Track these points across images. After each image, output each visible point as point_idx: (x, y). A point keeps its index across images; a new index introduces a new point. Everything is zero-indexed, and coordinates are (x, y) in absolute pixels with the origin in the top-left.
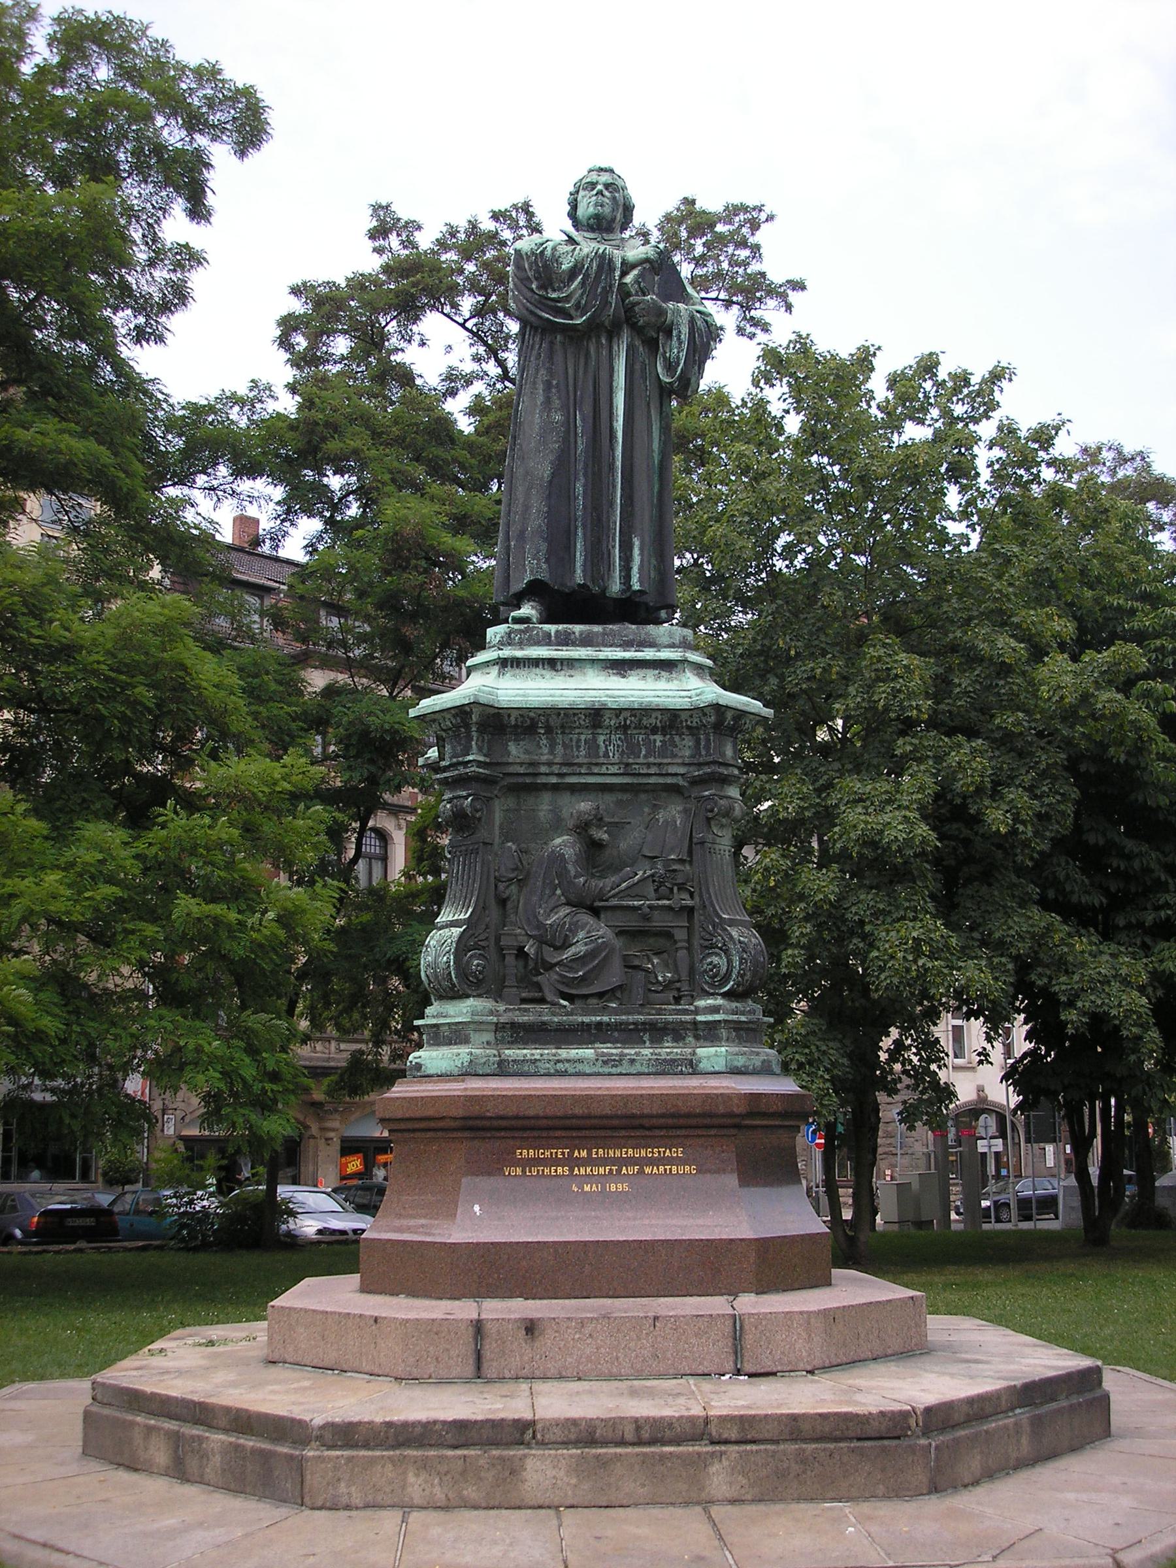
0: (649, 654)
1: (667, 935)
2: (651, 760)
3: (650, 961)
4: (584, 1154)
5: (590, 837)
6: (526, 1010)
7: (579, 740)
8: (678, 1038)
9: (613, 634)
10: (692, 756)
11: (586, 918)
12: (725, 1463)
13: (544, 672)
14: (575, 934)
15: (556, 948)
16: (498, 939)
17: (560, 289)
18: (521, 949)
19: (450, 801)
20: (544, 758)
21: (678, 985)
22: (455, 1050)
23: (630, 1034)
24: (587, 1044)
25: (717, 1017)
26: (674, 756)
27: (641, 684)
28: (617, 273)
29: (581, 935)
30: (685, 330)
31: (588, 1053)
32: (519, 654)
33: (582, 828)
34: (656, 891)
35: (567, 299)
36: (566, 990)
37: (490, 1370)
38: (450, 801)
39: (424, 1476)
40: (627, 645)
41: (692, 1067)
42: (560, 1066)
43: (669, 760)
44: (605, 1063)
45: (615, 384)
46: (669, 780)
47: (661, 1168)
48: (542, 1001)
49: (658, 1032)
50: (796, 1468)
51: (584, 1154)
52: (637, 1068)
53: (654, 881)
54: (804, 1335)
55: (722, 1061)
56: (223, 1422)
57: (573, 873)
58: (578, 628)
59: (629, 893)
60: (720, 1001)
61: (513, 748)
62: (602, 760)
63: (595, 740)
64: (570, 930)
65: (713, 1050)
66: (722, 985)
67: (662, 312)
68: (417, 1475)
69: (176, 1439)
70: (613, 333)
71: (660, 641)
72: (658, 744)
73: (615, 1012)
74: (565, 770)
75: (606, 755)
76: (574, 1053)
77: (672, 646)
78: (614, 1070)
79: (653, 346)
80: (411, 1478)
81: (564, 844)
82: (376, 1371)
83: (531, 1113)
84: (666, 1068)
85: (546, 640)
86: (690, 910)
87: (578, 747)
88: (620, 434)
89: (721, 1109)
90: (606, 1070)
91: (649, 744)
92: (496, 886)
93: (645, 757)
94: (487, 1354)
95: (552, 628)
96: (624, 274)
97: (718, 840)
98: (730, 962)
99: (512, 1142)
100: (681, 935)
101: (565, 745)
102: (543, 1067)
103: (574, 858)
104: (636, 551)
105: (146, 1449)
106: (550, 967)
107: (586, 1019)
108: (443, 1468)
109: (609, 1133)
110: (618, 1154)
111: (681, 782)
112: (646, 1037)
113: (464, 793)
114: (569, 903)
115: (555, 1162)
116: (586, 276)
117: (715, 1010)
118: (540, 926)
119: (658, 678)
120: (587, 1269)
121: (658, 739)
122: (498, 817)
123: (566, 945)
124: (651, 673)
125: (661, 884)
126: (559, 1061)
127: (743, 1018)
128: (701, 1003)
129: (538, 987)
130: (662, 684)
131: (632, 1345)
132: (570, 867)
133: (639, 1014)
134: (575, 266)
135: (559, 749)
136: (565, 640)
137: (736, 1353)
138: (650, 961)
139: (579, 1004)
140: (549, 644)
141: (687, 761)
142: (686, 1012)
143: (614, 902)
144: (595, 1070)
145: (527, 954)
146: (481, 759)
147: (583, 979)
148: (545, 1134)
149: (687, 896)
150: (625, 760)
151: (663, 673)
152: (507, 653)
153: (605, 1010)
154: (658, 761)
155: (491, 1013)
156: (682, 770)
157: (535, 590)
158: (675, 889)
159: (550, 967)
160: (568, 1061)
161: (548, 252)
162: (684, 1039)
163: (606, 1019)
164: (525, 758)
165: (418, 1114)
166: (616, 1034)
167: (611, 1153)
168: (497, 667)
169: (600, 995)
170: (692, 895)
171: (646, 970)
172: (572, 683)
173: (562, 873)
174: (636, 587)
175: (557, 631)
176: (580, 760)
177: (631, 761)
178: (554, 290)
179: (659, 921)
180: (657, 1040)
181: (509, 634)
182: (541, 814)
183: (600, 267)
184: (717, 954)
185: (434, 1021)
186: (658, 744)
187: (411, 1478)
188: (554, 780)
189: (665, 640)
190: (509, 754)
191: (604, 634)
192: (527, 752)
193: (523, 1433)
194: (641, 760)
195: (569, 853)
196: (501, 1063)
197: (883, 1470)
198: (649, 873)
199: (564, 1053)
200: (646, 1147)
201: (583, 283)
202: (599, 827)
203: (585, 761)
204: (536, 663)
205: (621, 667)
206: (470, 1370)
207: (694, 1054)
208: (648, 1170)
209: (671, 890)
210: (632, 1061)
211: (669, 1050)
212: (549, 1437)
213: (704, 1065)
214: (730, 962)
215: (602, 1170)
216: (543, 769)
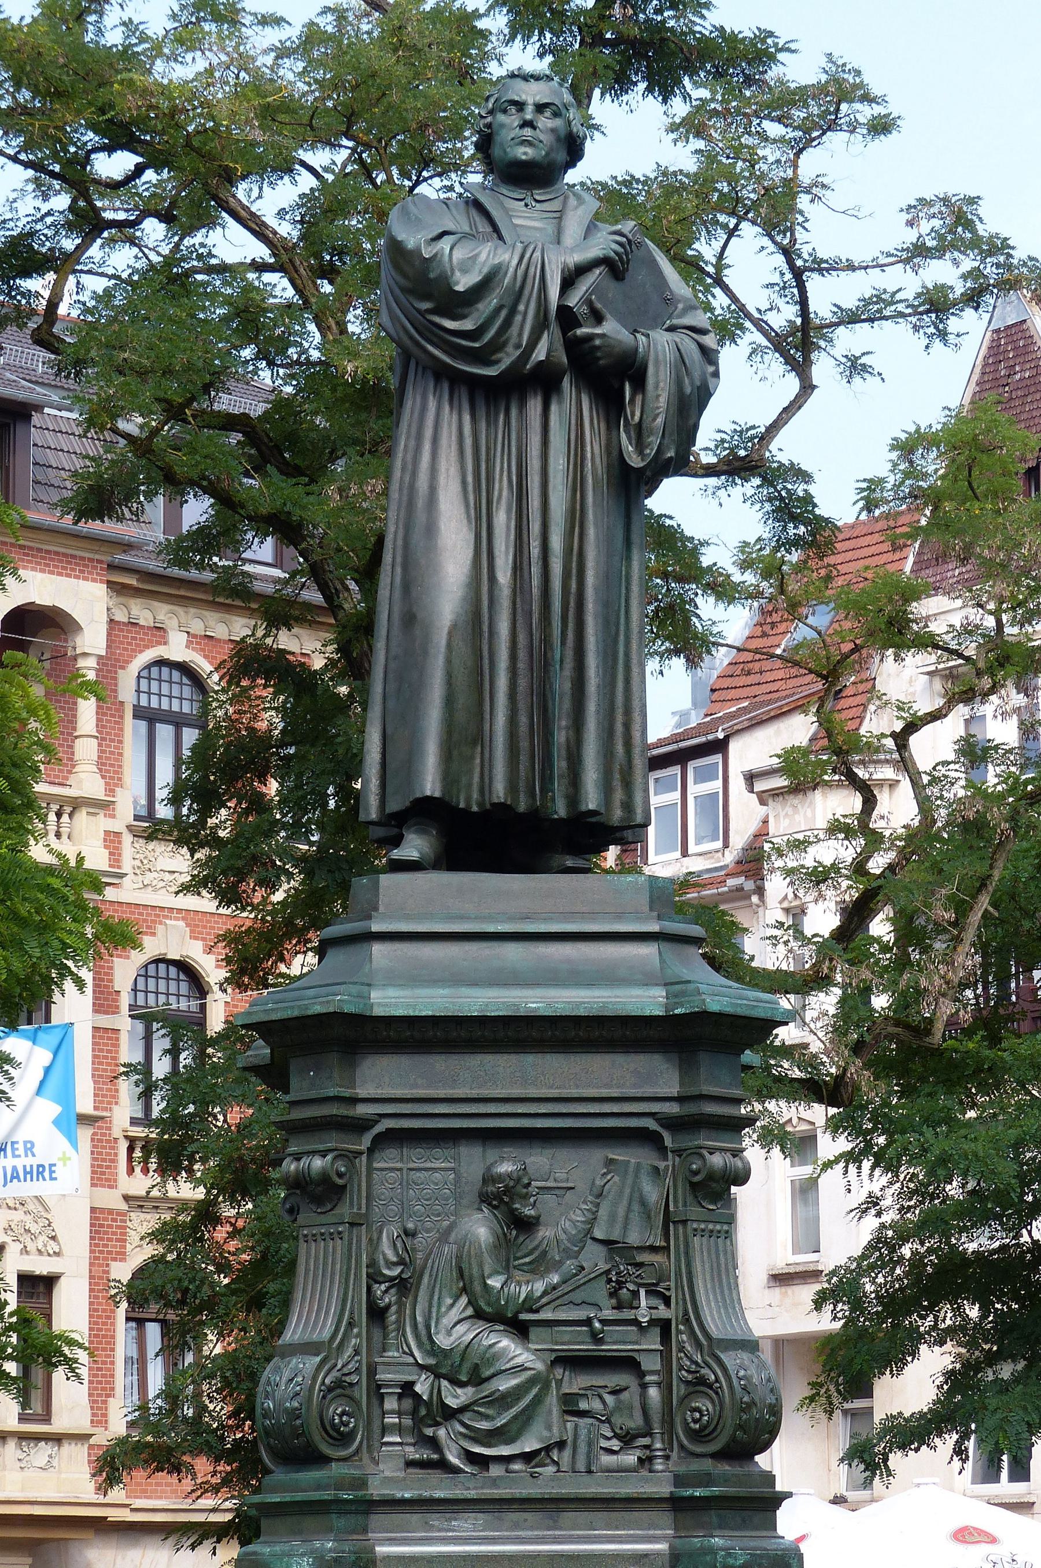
1: (629, 1363)
16: (372, 1371)
18: (407, 1388)
21: (646, 1441)
34: (613, 1294)
36: (478, 1449)
53: (610, 1281)
86: (665, 1326)
92: (369, 1289)
100: (651, 1363)
106: (450, 1414)
111: (651, 1124)
125: (620, 1284)
129: (433, 1443)
145: (417, 1396)
157: (424, 811)
158: (642, 1292)
159: (450, 1414)
169: (527, 1457)
209: (635, 1294)
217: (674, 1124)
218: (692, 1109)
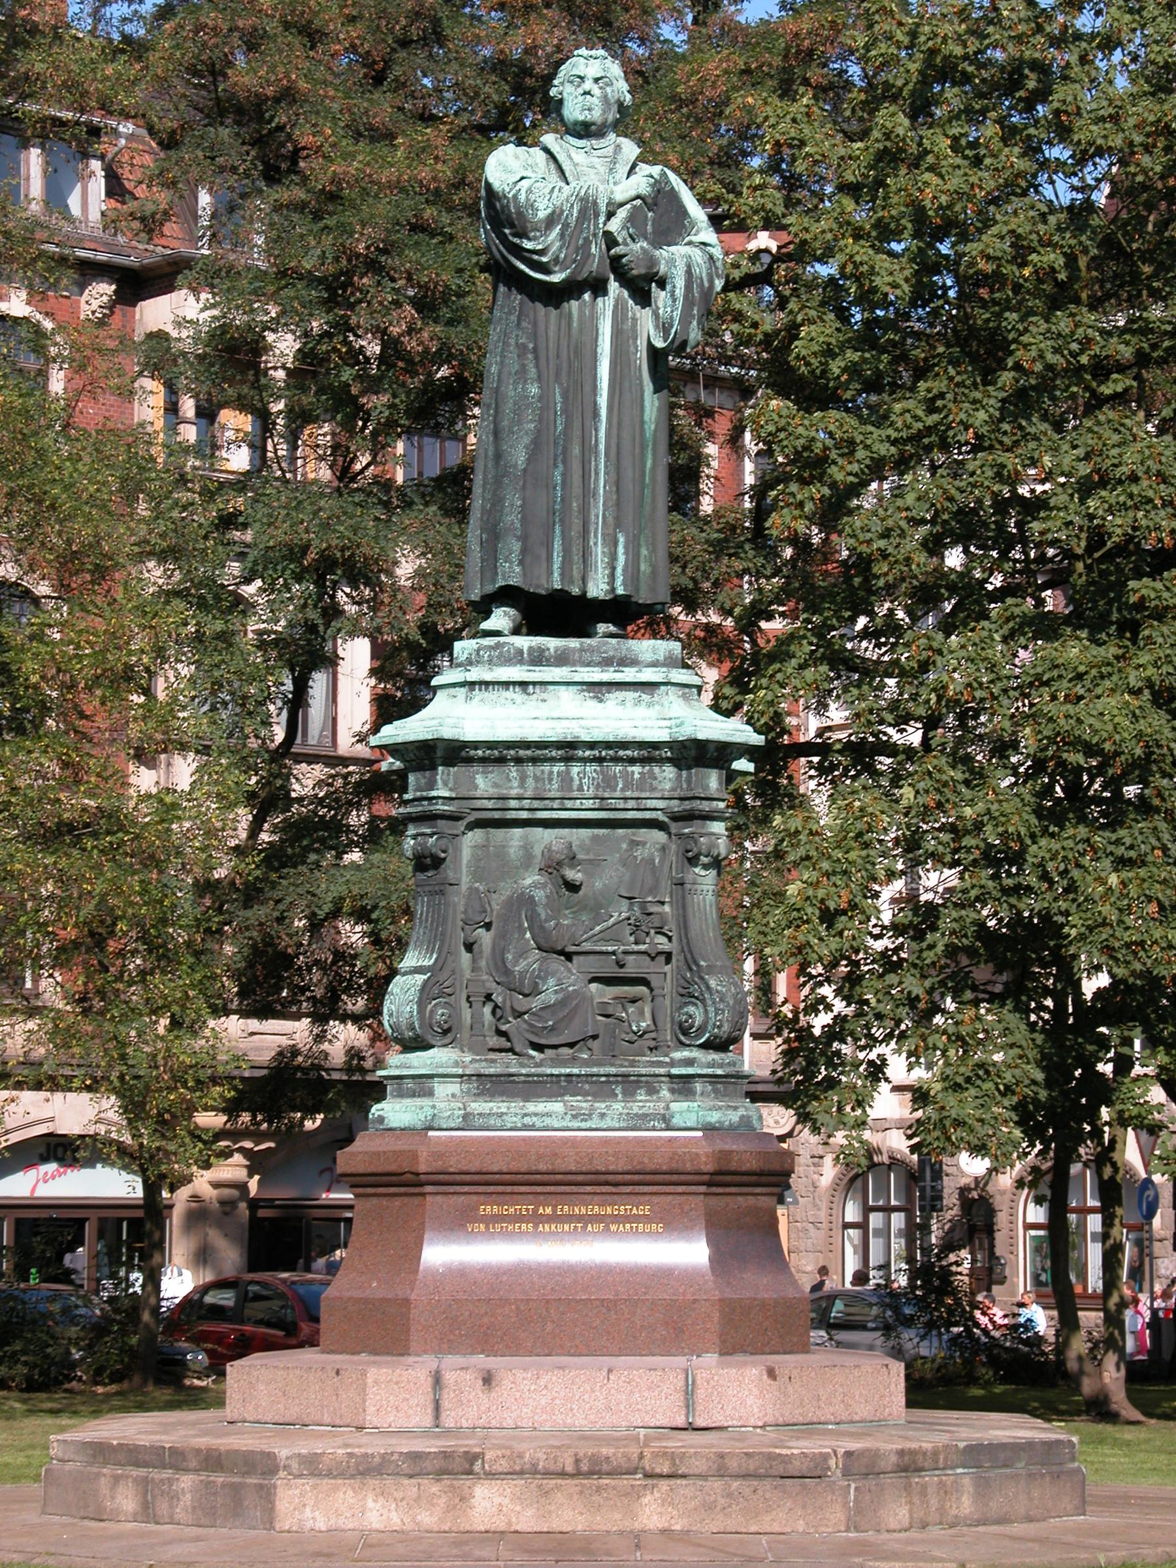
0: (629, 674)
2: (628, 794)
3: (625, 1009)
4: (549, 1211)
5: (563, 877)
6: (493, 1061)
7: (551, 773)
8: (652, 1091)
9: (591, 649)
10: (673, 790)
11: (557, 963)
12: (657, 1495)
13: (515, 696)
14: (545, 980)
15: (525, 995)
17: (535, 239)
19: (414, 837)
20: (514, 792)
22: (418, 1101)
23: (602, 1088)
24: (556, 1096)
25: (690, 1071)
26: (653, 789)
27: (619, 711)
28: (602, 219)
29: (551, 982)
30: (680, 283)
31: (557, 1107)
32: (488, 677)
33: (552, 867)
35: (542, 252)
36: (535, 1040)
37: (448, 1421)
38: (414, 837)
39: (381, 1500)
40: (606, 663)
41: (667, 1123)
42: (527, 1120)
43: (647, 795)
44: (574, 1117)
45: (599, 350)
46: (648, 815)
47: (628, 1226)
48: (511, 1050)
49: (630, 1084)
50: (722, 1501)
51: (549, 1211)
52: (607, 1122)
54: (756, 1391)
55: (693, 1117)
56: (193, 1464)
57: (543, 917)
58: (552, 643)
59: (604, 937)
60: (696, 1054)
61: (480, 780)
62: (575, 794)
63: (568, 772)
64: (538, 977)
65: (685, 1105)
66: (698, 1037)
67: (653, 262)
68: (375, 1501)
69: (144, 1485)
70: (598, 288)
71: (642, 657)
72: (637, 776)
73: (586, 1063)
74: (536, 804)
75: (580, 789)
76: (541, 1107)
77: (654, 664)
78: (583, 1125)
79: (643, 298)
80: (370, 1503)
81: (535, 885)
82: (338, 1422)
83: (495, 1169)
84: (639, 1121)
85: (517, 658)
87: (551, 780)
88: (603, 413)
89: (689, 1167)
90: (576, 1124)
91: (626, 776)
93: (622, 790)
94: (445, 1404)
95: (524, 642)
96: (610, 215)
97: (700, 880)
98: (706, 1012)
99: (474, 1198)
101: (536, 778)
102: (510, 1121)
103: (544, 901)
104: (621, 550)
105: (113, 1498)
107: (555, 1071)
108: (399, 1495)
109: (574, 1189)
110: (583, 1211)
111: (660, 816)
112: (618, 1090)
113: (428, 831)
114: (539, 949)
115: (519, 1219)
116: (566, 226)
117: (690, 1062)
118: (507, 972)
119: (638, 702)
120: (549, 1327)
121: (636, 769)
122: (466, 854)
123: (535, 992)
124: (630, 695)
126: (526, 1115)
127: (719, 1072)
128: (677, 1055)
130: (642, 711)
131: (586, 1397)
132: (540, 910)
133: (612, 1065)
134: (554, 212)
135: (530, 782)
136: (538, 658)
137: (687, 1407)
138: (625, 1009)
139: (549, 1053)
140: (521, 662)
141: (667, 794)
142: (660, 1064)
143: (587, 946)
144: (564, 1124)
146: (447, 794)
147: (553, 1029)
148: (509, 1189)
149: (665, 940)
150: (600, 794)
151: (644, 696)
152: (475, 674)
153: (574, 1060)
154: (636, 794)
155: (456, 1064)
156: (661, 804)
160: (536, 1115)
161: (522, 197)
162: (658, 1092)
163: (576, 1071)
164: (492, 791)
165: (380, 1170)
166: (587, 1086)
167: (577, 1210)
168: (463, 690)
169: (571, 1045)
170: (670, 938)
171: (621, 1020)
172: (544, 710)
173: (533, 918)
174: (620, 591)
175: (530, 648)
176: (552, 794)
177: (606, 795)
178: (529, 239)
179: (633, 967)
180: (629, 1094)
181: (478, 651)
182: (512, 851)
183: (583, 213)
184: (695, 1004)
185: (397, 1072)
186: (637, 776)
187: (370, 1503)
188: (524, 815)
189: (648, 657)
190: (476, 787)
191: (582, 650)
192: (496, 785)
193: (472, 1464)
194: (618, 794)
195: (539, 895)
196: (466, 1117)
197: (804, 1507)
198: (624, 915)
199: (531, 1107)
200: (612, 1204)
201: (562, 235)
202: (572, 867)
203: (558, 795)
204: (506, 684)
205: (598, 689)
206: (428, 1420)
207: (668, 1108)
208: (613, 1227)
210: (603, 1115)
211: (642, 1103)
212: (497, 1468)
213: (676, 1121)
214: (706, 1012)
215: (566, 1227)
216: (513, 804)
217: (676, 818)
218: (687, 805)
